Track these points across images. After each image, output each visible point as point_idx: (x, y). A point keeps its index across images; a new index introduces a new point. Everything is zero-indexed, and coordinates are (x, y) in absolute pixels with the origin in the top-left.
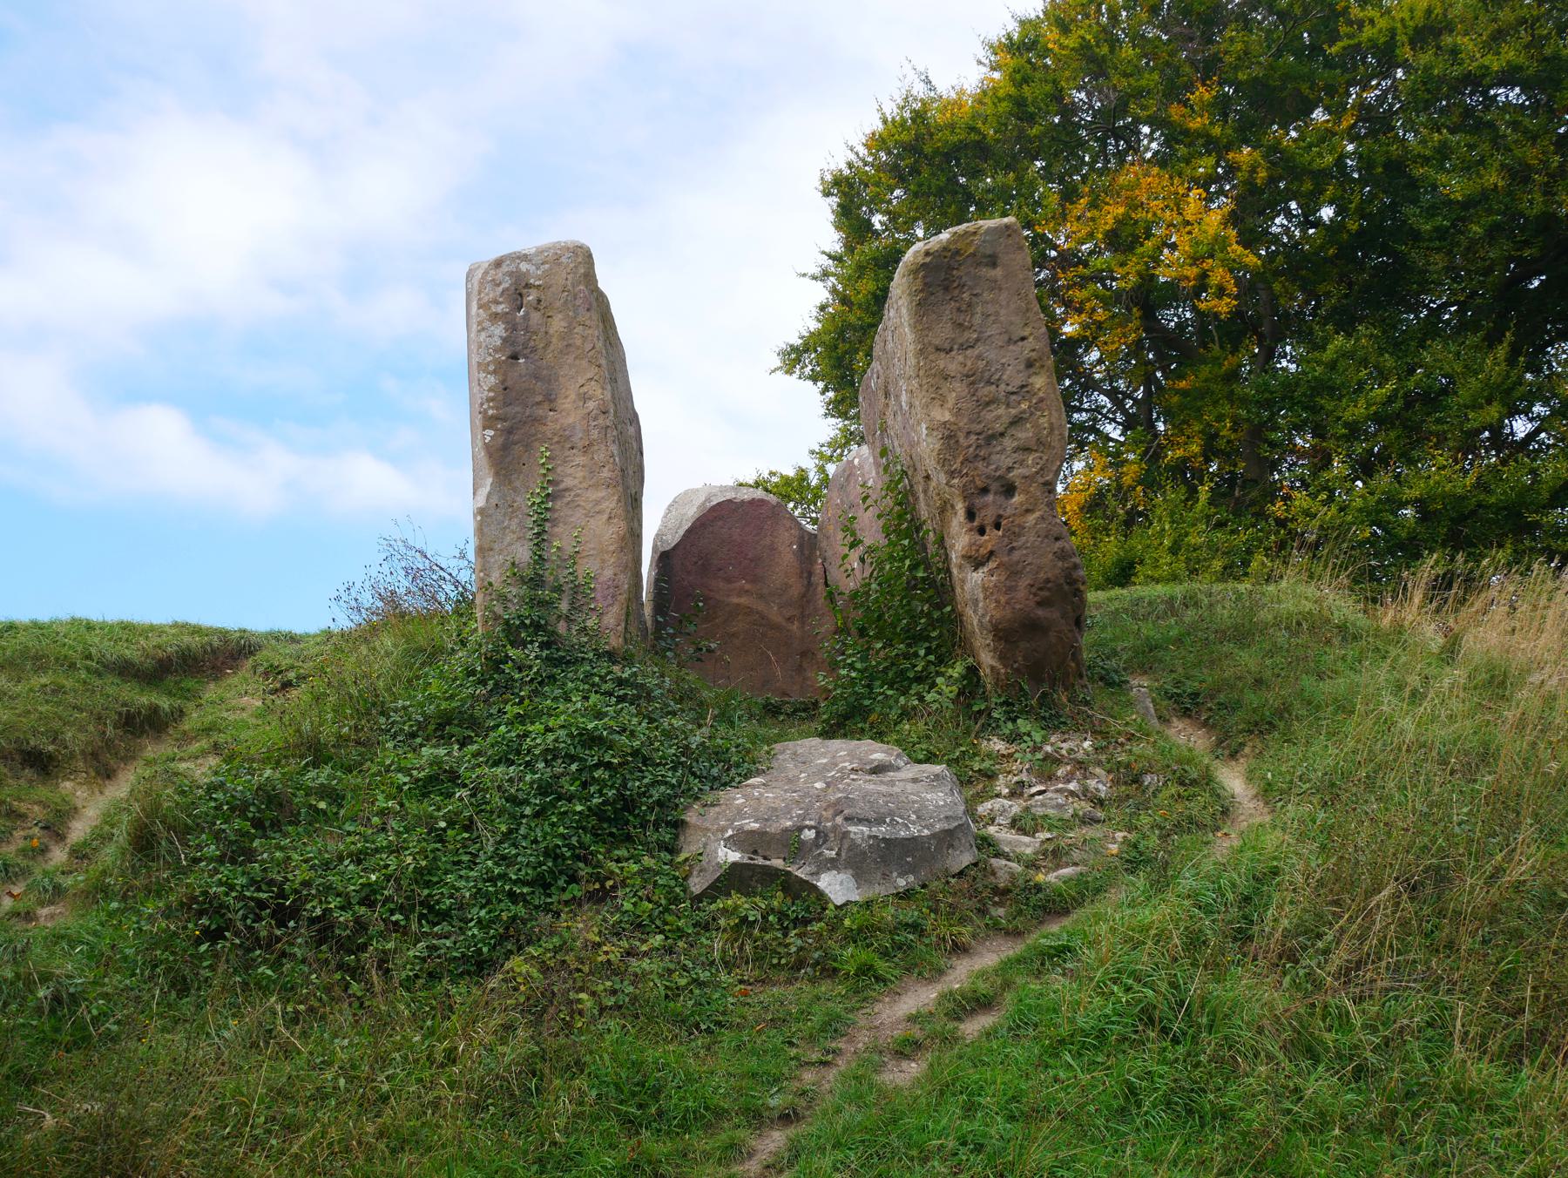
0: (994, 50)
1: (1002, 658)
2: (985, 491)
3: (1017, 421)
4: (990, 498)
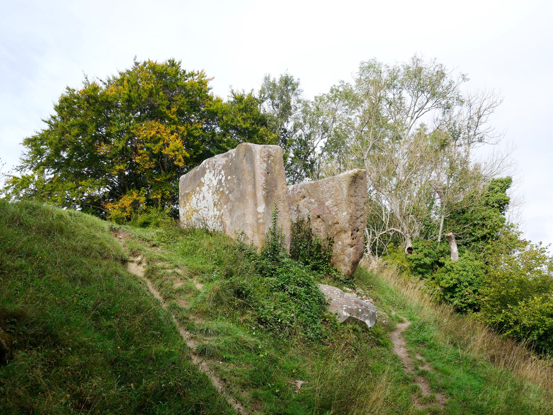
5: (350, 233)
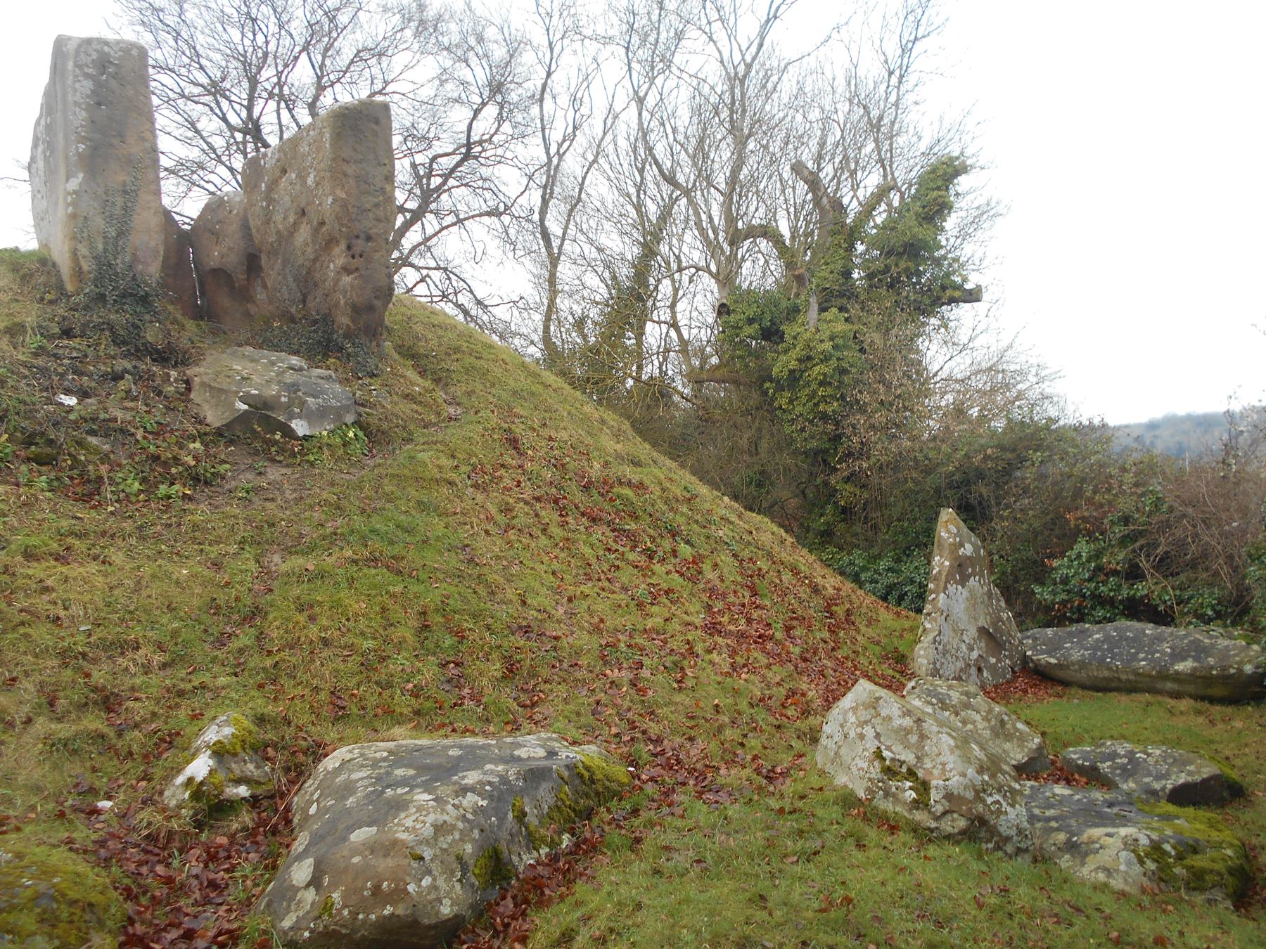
0: (943, 174)
1: (353, 321)
2: (357, 237)
3: (377, 205)
4: (359, 241)
5: (343, 246)
